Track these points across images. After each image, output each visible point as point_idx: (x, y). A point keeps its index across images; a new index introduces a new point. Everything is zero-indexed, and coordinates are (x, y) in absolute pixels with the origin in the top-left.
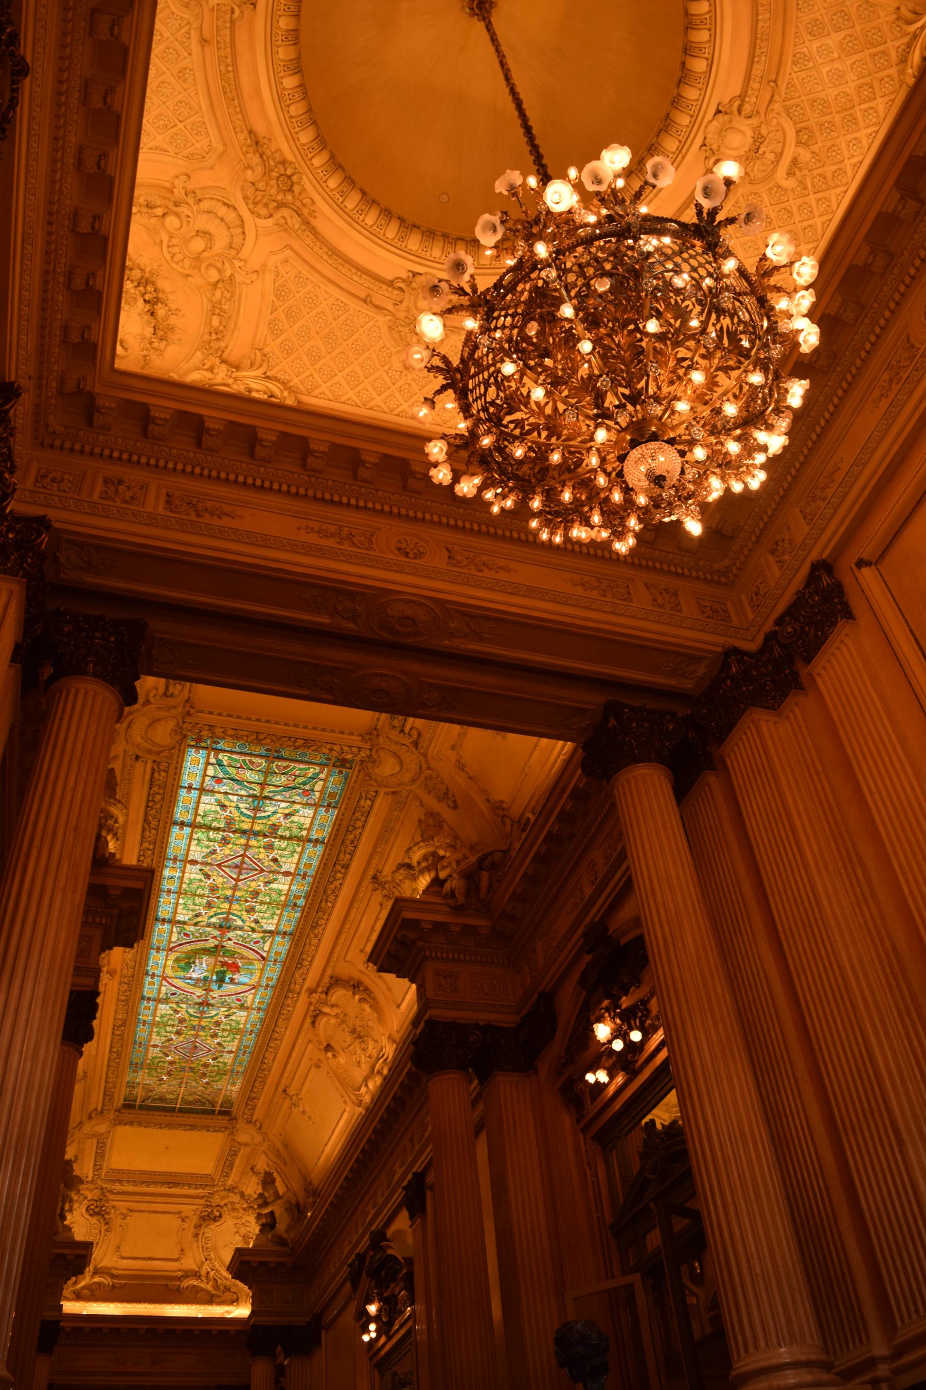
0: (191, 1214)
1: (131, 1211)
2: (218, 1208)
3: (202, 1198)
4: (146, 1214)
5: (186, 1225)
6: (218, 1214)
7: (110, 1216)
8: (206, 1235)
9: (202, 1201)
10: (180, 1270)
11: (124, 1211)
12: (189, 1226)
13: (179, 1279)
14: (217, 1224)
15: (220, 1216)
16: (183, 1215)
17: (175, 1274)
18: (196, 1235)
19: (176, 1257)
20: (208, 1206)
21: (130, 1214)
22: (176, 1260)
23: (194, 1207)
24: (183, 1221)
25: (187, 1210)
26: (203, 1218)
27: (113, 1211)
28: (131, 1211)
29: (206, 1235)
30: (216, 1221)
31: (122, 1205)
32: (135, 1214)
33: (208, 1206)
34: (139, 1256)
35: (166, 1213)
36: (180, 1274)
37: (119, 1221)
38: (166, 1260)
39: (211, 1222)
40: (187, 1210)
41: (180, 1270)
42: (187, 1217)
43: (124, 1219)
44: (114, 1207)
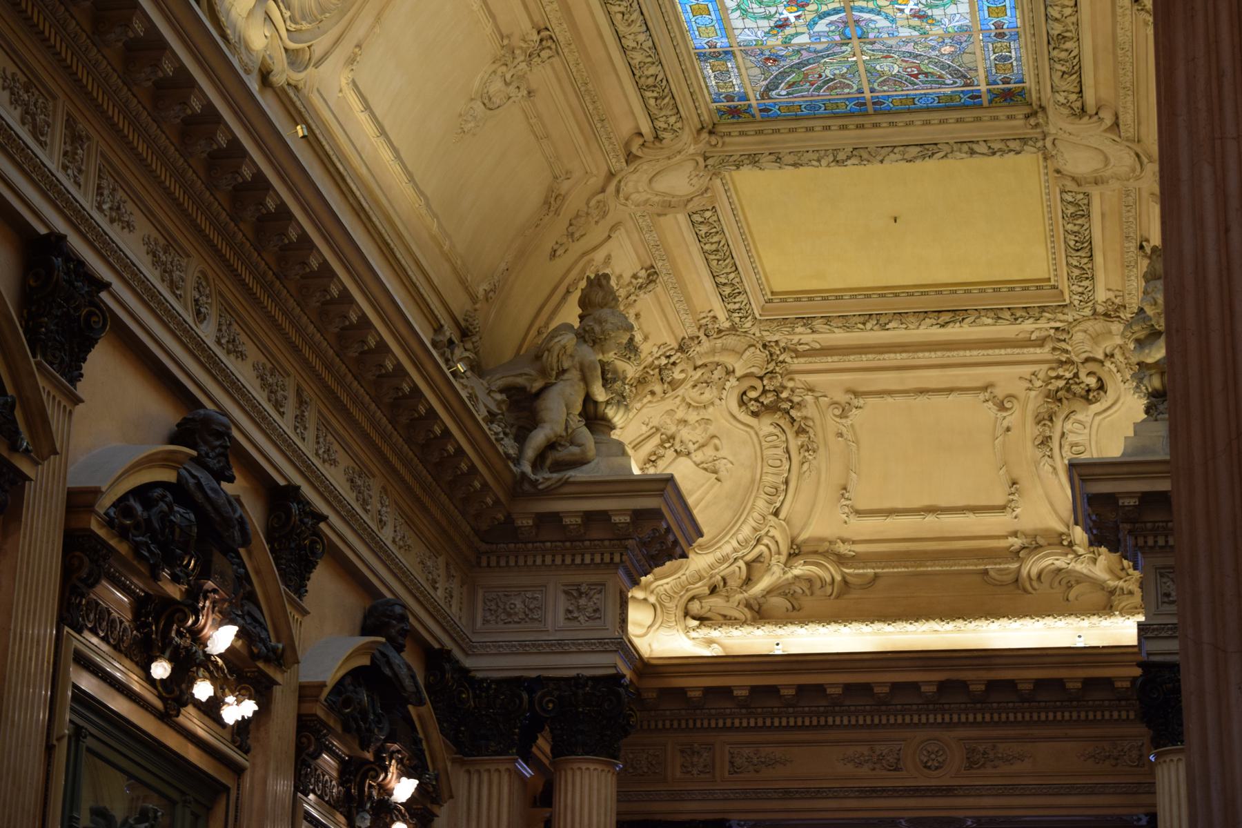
0: (1019, 388)
1: (856, 394)
2: (1091, 366)
3: (1041, 342)
4: (900, 400)
5: (1012, 419)
6: (1092, 381)
7: (804, 413)
8: (1071, 438)
9: (1044, 353)
10: (1015, 534)
11: (843, 398)
12: (1021, 419)
13: (1016, 554)
14: (1096, 408)
15: (1102, 387)
16: (1000, 392)
17: (1003, 543)
18: (1045, 441)
19: (1000, 501)
20: (1061, 363)
21: (855, 402)
22: (1002, 508)
23: (1026, 370)
24: (1002, 407)
25: (1007, 379)
26: (1055, 397)
27: (809, 398)
28: (856, 394)
29: (1071, 438)
30: (1090, 402)
31: (832, 383)
32: (871, 401)
33: (1061, 363)
34: (900, 505)
35: (951, 390)
36: (1016, 542)
37: (832, 423)
38: (974, 509)
39: (1078, 404)
40: (1007, 379)
41: (1015, 534)
42: (1011, 396)
43: (843, 415)
44: (811, 390)
